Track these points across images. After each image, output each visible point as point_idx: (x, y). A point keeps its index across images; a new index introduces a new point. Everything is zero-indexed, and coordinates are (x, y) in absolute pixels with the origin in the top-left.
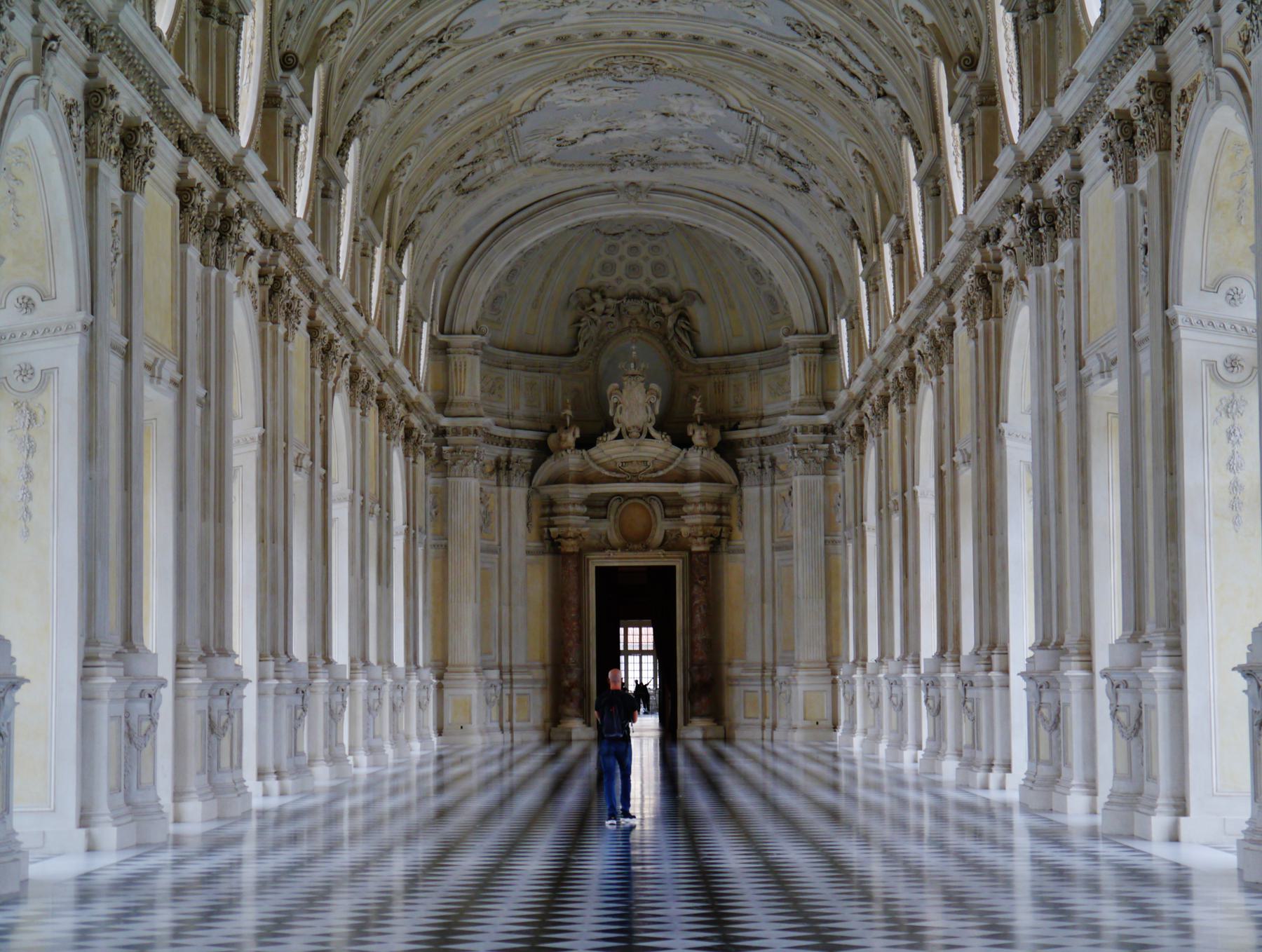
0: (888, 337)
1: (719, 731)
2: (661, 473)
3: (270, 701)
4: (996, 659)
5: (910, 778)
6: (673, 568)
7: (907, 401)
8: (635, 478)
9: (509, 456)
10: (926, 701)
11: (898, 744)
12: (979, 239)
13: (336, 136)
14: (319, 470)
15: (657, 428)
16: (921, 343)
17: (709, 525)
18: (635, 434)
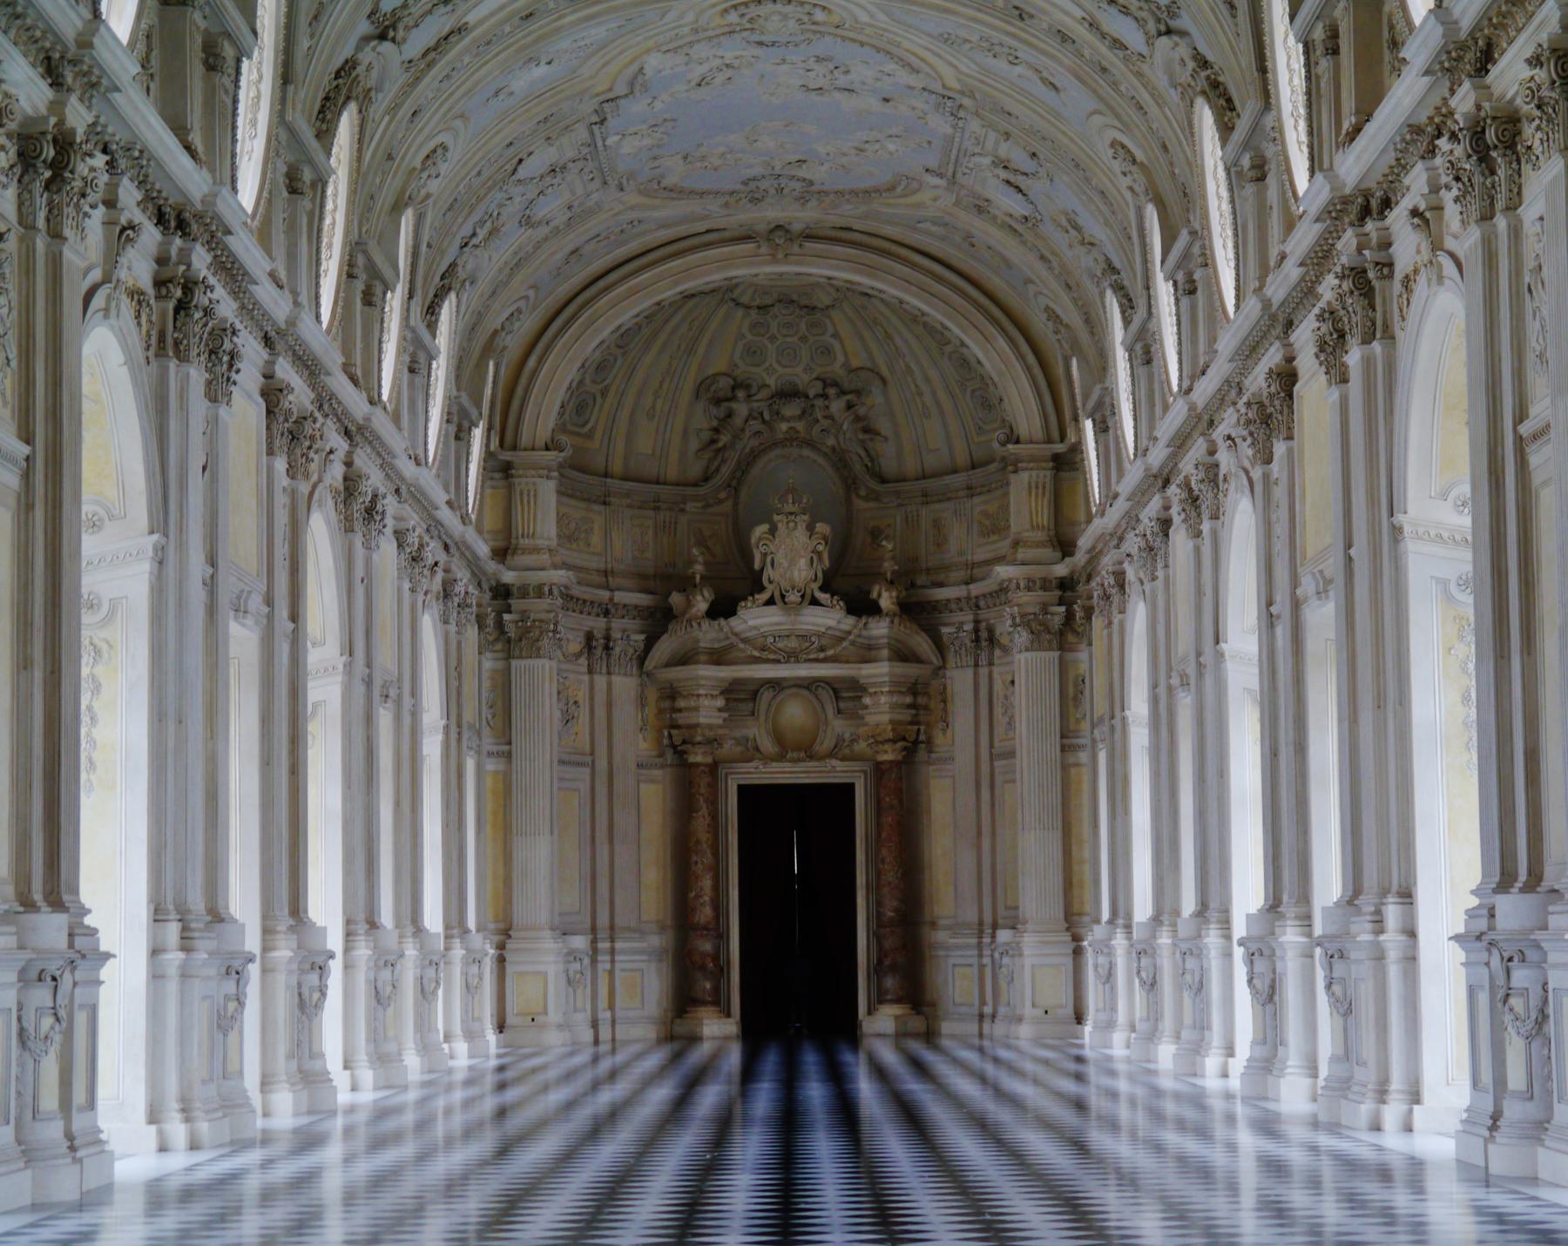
0: (1169, 425)
1: (917, 1024)
2: (830, 652)
3: (172, 987)
4: (1392, 913)
5: (1217, 1104)
6: (849, 789)
7: (1205, 516)
8: (792, 657)
9: (608, 629)
10: (1329, 986)
11: (1196, 1050)
12: (1354, 209)
13: (308, 94)
14: (284, 624)
15: (823, 589)
16: (1228, 422)
17: (900, 723)
18: (793, 597)
